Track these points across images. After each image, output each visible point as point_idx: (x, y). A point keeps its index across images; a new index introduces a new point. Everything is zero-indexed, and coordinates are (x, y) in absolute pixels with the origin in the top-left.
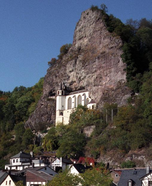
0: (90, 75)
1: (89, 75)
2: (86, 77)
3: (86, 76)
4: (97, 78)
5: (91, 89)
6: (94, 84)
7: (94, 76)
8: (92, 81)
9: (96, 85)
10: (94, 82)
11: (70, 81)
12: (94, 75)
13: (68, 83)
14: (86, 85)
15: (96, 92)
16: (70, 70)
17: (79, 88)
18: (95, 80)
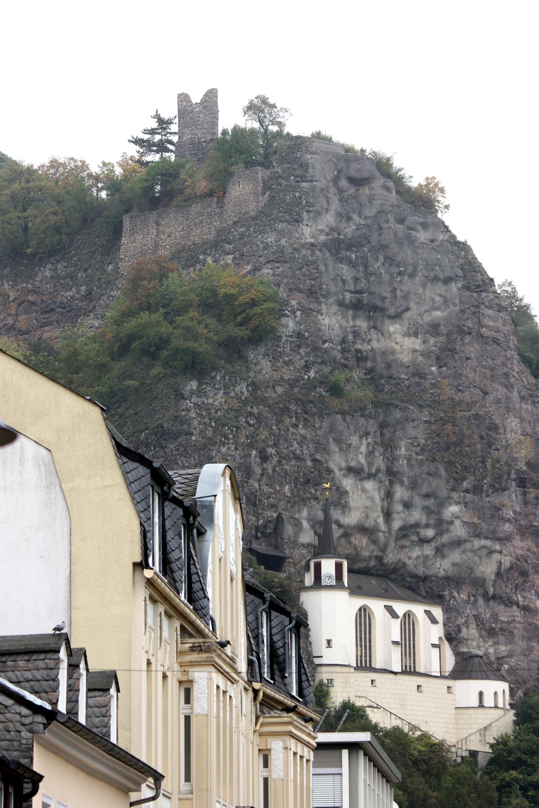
0: (488, 543)
1: (483, 542)
2: (468, 545)
3: (466, 541)
4: (511, 568)
5: (468, 602)
6: (495, 589)
7: (496, 557)
8: (487, 569)
9: (501, 598)
10: (495, 581)
11: (351, 519)
12: (501, 552)
13: (340, 526)
14: (447, 578)
15: (501, 629)
16: (353, 464)
17: (372, 563)
18: (498, 574)
